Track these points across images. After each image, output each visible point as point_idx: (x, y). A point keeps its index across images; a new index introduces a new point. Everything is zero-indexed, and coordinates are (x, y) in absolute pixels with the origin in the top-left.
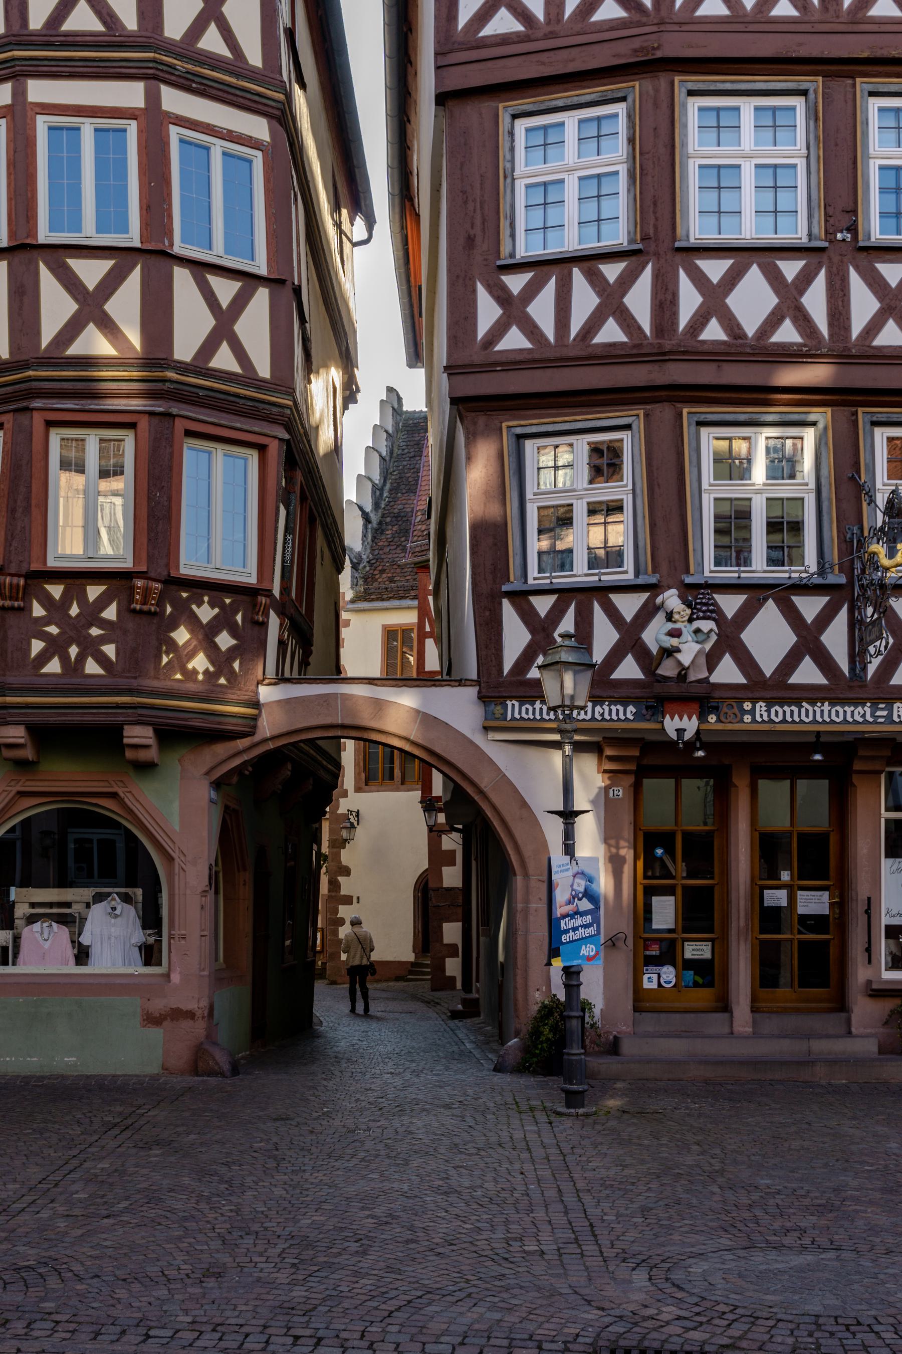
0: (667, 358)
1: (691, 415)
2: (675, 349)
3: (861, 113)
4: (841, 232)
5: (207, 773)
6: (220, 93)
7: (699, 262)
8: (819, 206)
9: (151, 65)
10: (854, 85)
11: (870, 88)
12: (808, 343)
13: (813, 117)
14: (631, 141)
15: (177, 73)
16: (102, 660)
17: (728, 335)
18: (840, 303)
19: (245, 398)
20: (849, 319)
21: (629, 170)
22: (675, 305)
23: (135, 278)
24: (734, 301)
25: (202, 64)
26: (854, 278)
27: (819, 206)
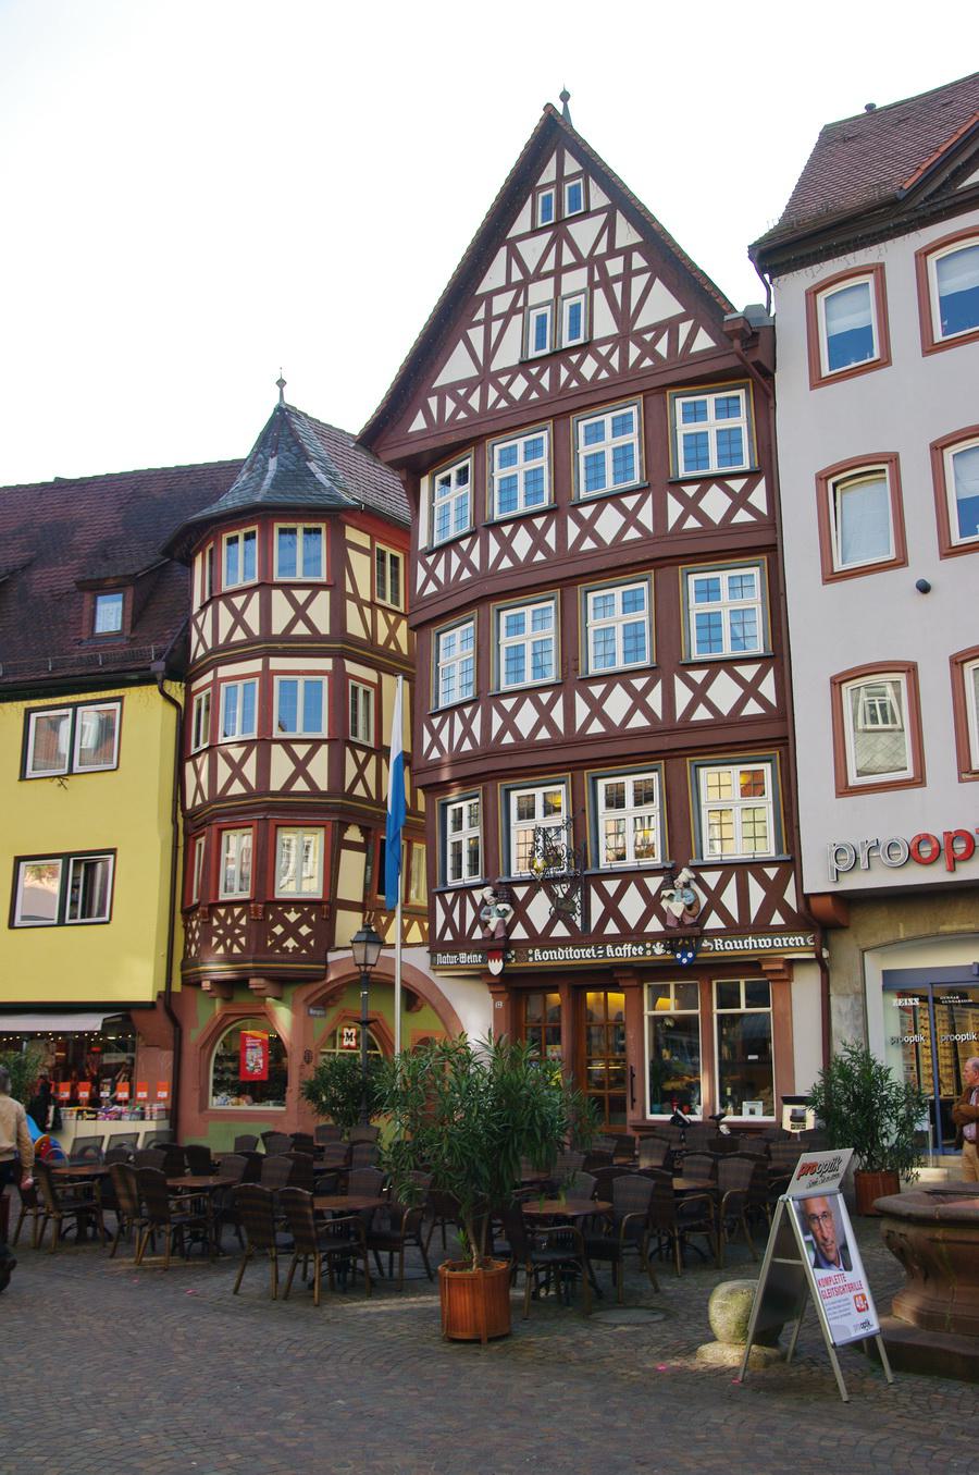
5: (306, 1000)
16: (240, 945)
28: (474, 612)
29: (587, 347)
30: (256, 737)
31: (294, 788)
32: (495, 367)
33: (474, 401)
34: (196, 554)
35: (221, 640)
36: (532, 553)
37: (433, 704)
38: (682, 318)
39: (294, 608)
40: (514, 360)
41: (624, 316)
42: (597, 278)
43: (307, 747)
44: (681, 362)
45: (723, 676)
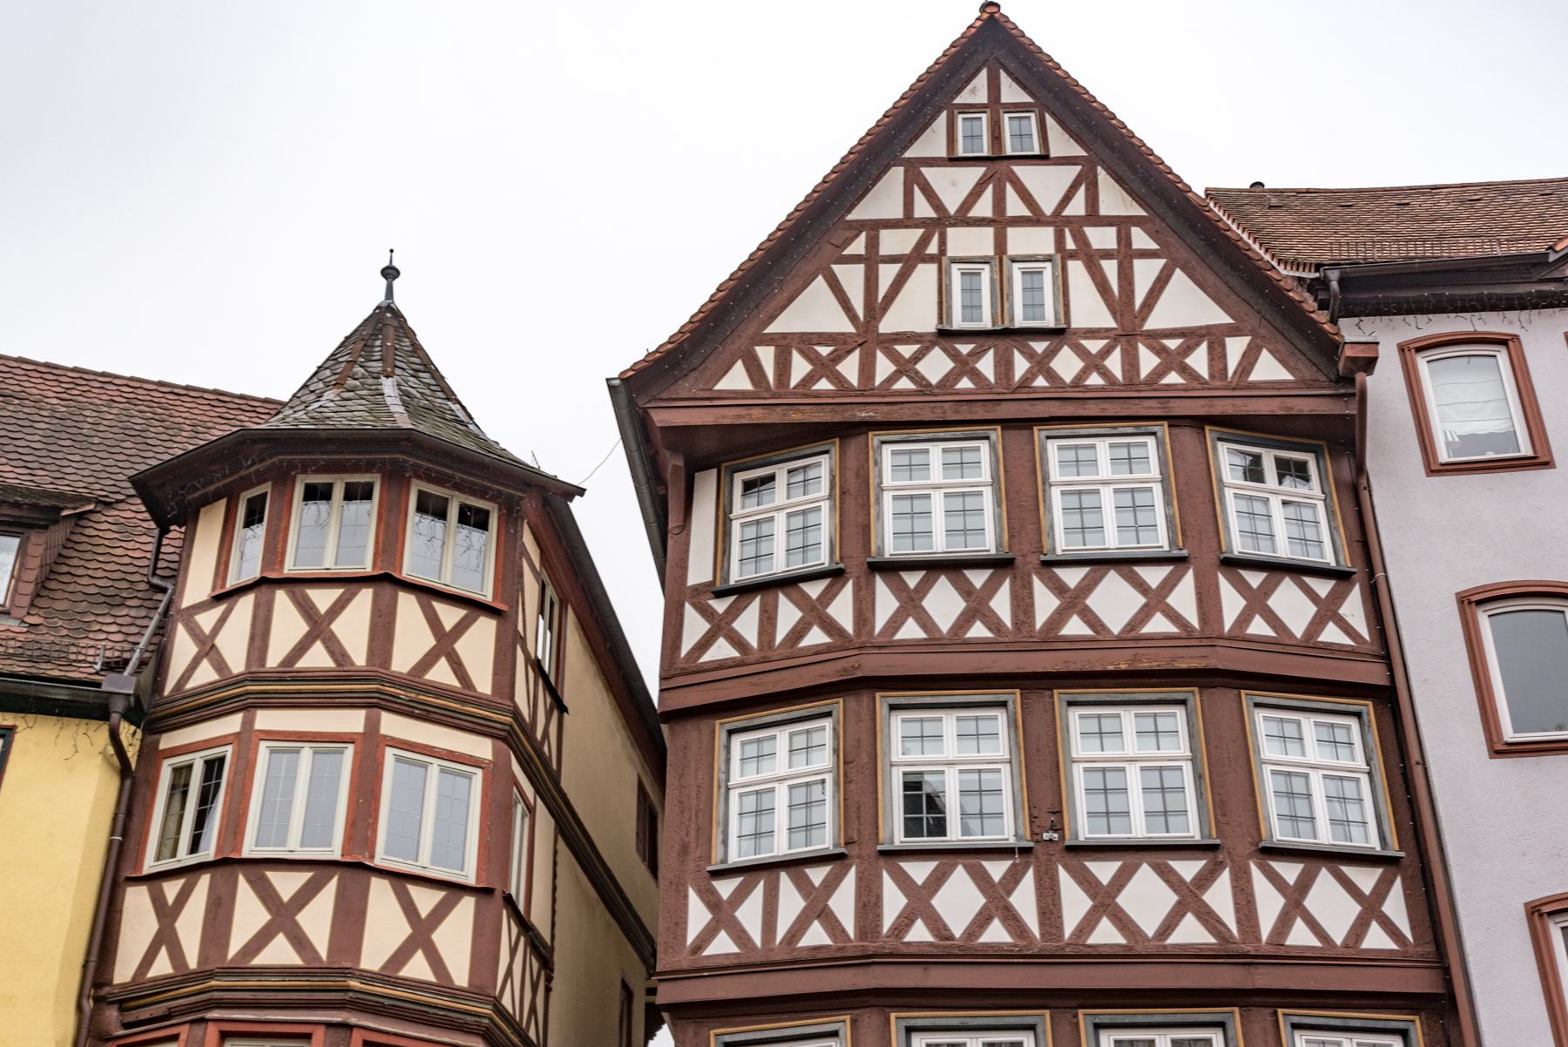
0: (870, 960)
1: (899, 1020)
2: (879, 951)
3: (1061, 720)
4: (1047, 832)
6: (442, 718)
7: (902, 864)
8: (1023, 808)
9: (377, 695)
10: (1052, 696)
11: (1069, 698)
12: (1019, 943)
13: (1012, 724)
14: (836, 751)
15: (400, 701)
17: (935, 936)
18: (1050, 902)
19: (436, 1007)
20: (1060, 917)
21: (834, 778)
22: (879, 907)
23: (331, 888)
24: (941, 902)
25: (427, 692)
26: (1064, 876)
27: (1023, 808)
28: (838, 705)
29: (1058, 335)
30: (336, 855)
31: (406, 972)
32: (889, 324)
33: (850, 368)
34: (208, 500)
35: (273, 660)
36: (965, 620)
37: (717, 854)
38: (1234, 331)
39: (435, 635)
40: (929, 325)
41: (1120, 303)
42: (1070, 244)
43: (437, 896)
44: (1234, 389)
45: (1324, 879)
